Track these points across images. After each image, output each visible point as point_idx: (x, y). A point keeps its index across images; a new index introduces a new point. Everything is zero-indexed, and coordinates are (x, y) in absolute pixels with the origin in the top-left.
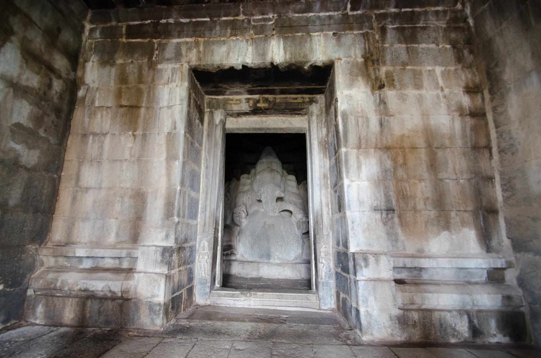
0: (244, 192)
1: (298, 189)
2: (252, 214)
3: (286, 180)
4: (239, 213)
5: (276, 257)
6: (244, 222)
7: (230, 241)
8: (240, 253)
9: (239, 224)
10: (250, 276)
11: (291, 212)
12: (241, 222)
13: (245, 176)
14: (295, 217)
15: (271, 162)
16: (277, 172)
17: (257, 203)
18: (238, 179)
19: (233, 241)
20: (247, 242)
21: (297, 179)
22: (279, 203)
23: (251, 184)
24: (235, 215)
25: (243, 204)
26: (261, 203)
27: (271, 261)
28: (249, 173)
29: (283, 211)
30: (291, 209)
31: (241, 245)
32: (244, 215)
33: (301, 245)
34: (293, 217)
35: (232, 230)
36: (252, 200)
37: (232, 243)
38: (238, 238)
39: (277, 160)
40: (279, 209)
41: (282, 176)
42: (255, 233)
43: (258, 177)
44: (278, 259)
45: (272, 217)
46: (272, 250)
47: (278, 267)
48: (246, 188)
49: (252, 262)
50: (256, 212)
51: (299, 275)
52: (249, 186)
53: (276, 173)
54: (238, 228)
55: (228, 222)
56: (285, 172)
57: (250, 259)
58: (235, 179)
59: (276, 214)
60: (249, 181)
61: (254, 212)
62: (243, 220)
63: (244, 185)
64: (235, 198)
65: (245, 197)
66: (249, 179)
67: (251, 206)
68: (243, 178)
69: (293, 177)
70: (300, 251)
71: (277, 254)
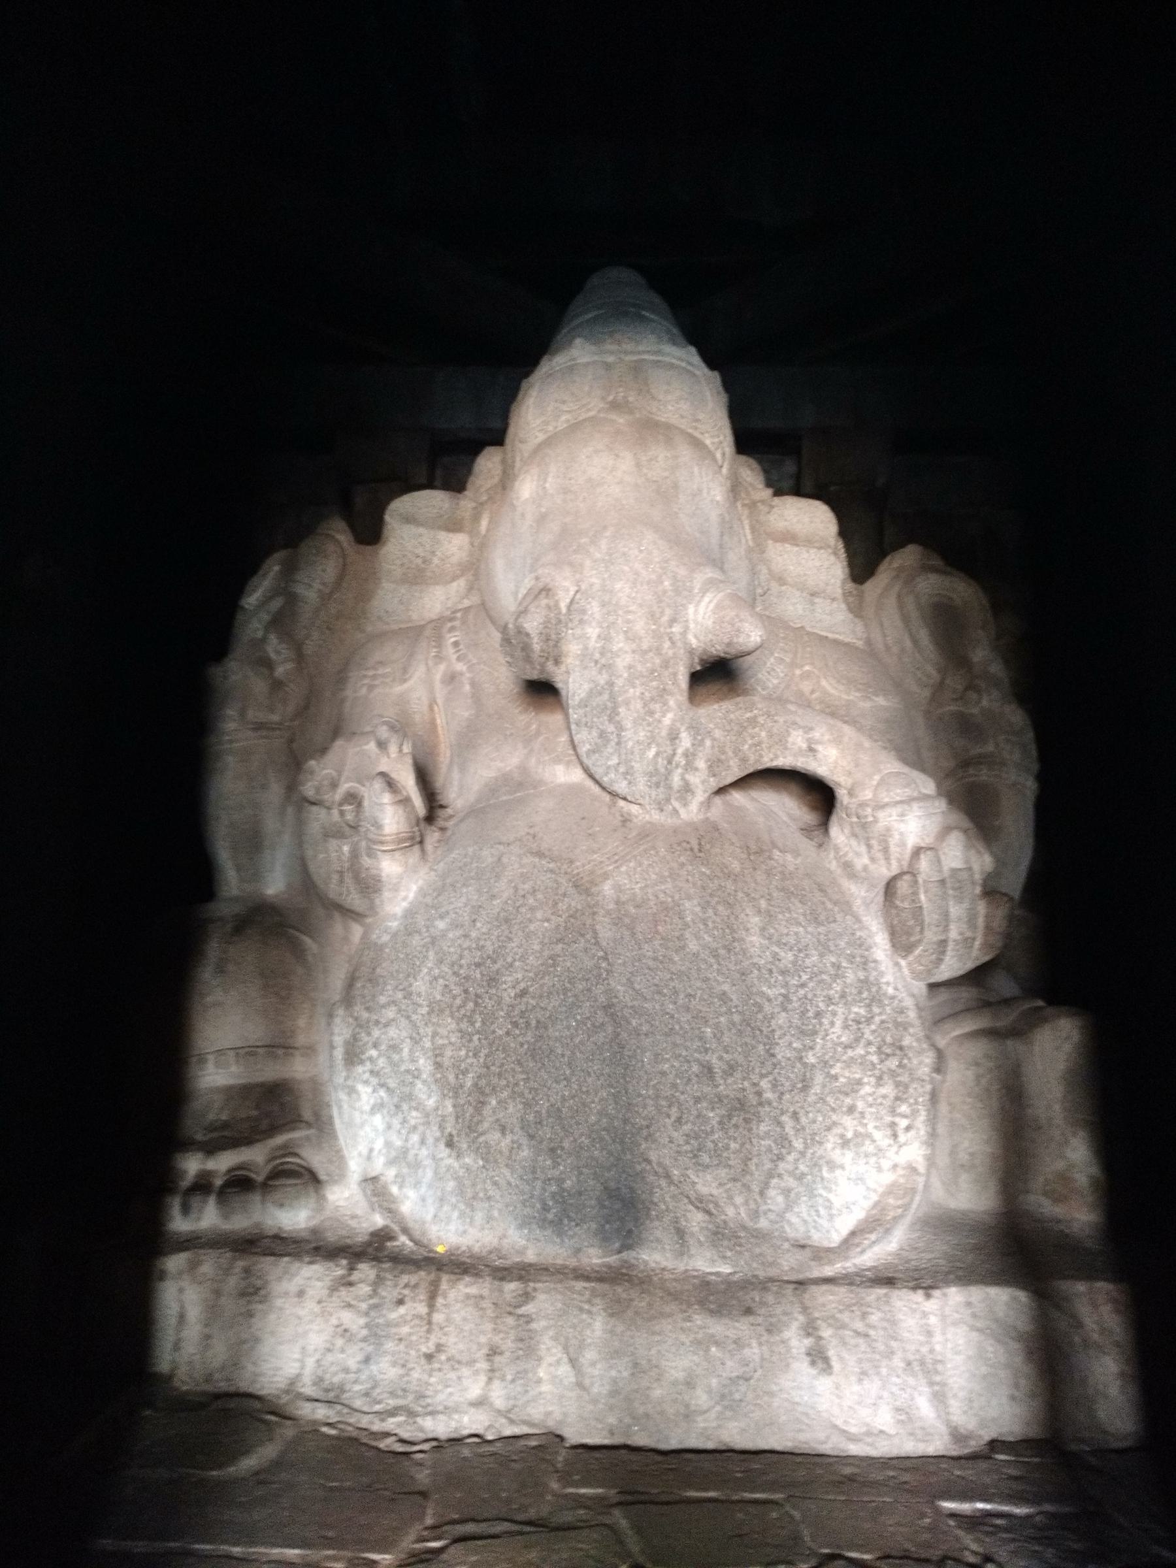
0: (414, 633)
1: (857, 609)
2: (476, 812)
3: (763, 536)
4: (353, 798)
5: (696, 1220)
6: (402, 885)
7: (280, 1046)
8: (355, 1167)
9: (354, 900)
10: (440, 1427)
11: (820, 795)
12: (370, 886)
13: (429, 502)
14: (862, 830)
15: (637, 369)
16: (697, 444)
17: (526, 719)
18: (370, 533)
19: (310, 1051)
20: (424, 1064)
21: (843, 533)
22: (717, 713)
23: (475, 569)
24: (318, 819)
25: (401, 727)
26: (554, 719)
27: (655, 1256)
28: (456, 483)
29: (746, 781)
30: (827, 763)
31: (366, 1095)
32: (391, 819)
33: (920, 1093)
34: (834, 830)
35: (298, 951)
36: (477, 697)
37: (298, 1069)
38: (341, 1033)
39: (690, 357)
40: (714, 765)
41: (735, 489)
42: (492, 981)
43: (526, 488)
44: (722, 1236)
45: (647, 834)
46: (658, 1155)
47: (717, 1327)
48: (436, 601)
49: (459, 1265)
50: (515, 789)
51: (925, 1408)
52: (460, 584)
53: (686, 453)
54: (357, 931)
55: (275, 884)
56: (751, 474)
57: (449, 1232)
58: (340, 534)
59: (691, 812)
60: (455, 546)
61: (492, 789)
62: (389, 867)
63: (418, 577)
64: (341, 679)
65: (418, 672)
66: (454, 526)
67: (468, 741)
68: (409, 520)
69: (814, 518)
70: (914, 1151)
71: (706, 1184)
